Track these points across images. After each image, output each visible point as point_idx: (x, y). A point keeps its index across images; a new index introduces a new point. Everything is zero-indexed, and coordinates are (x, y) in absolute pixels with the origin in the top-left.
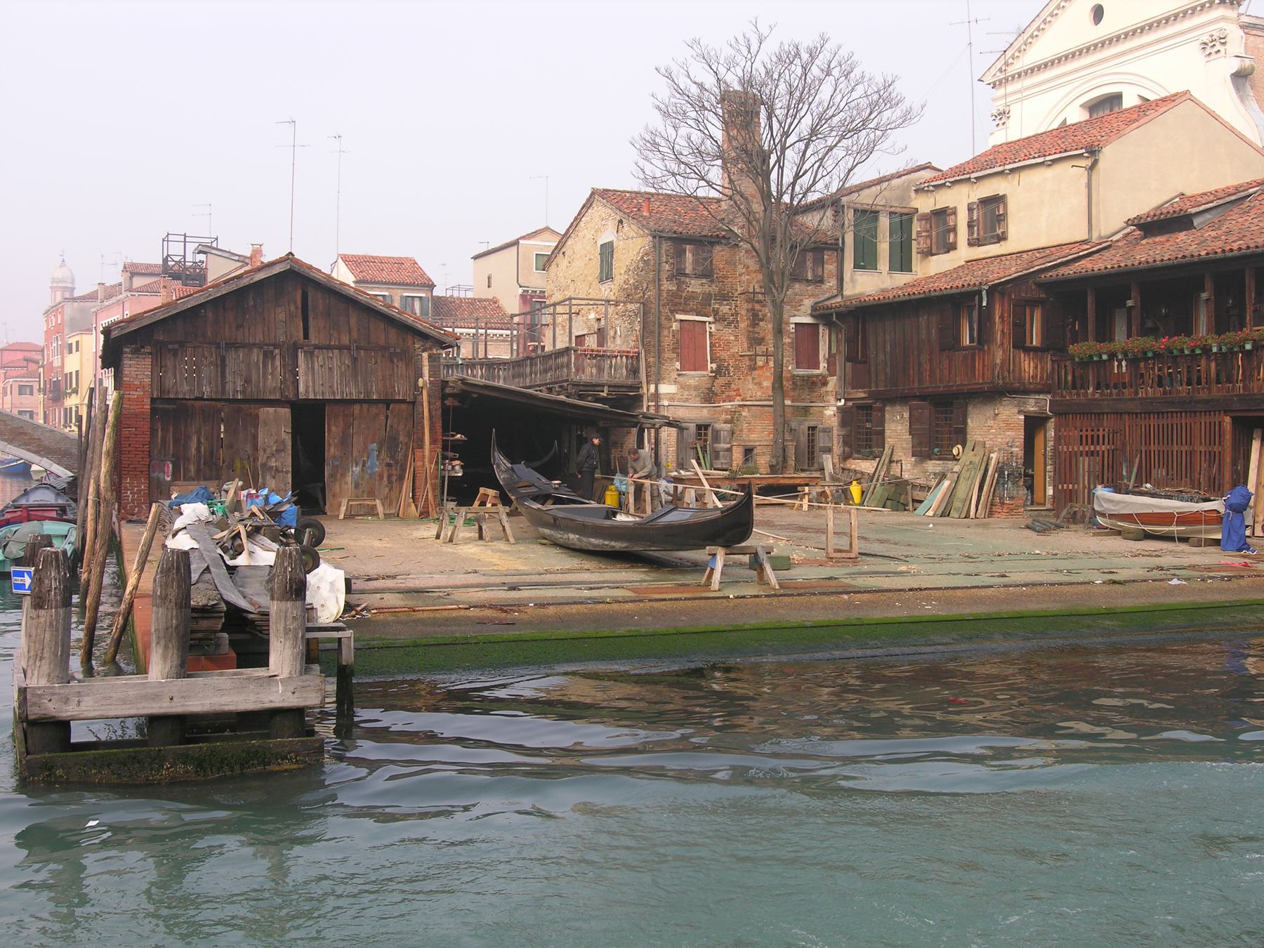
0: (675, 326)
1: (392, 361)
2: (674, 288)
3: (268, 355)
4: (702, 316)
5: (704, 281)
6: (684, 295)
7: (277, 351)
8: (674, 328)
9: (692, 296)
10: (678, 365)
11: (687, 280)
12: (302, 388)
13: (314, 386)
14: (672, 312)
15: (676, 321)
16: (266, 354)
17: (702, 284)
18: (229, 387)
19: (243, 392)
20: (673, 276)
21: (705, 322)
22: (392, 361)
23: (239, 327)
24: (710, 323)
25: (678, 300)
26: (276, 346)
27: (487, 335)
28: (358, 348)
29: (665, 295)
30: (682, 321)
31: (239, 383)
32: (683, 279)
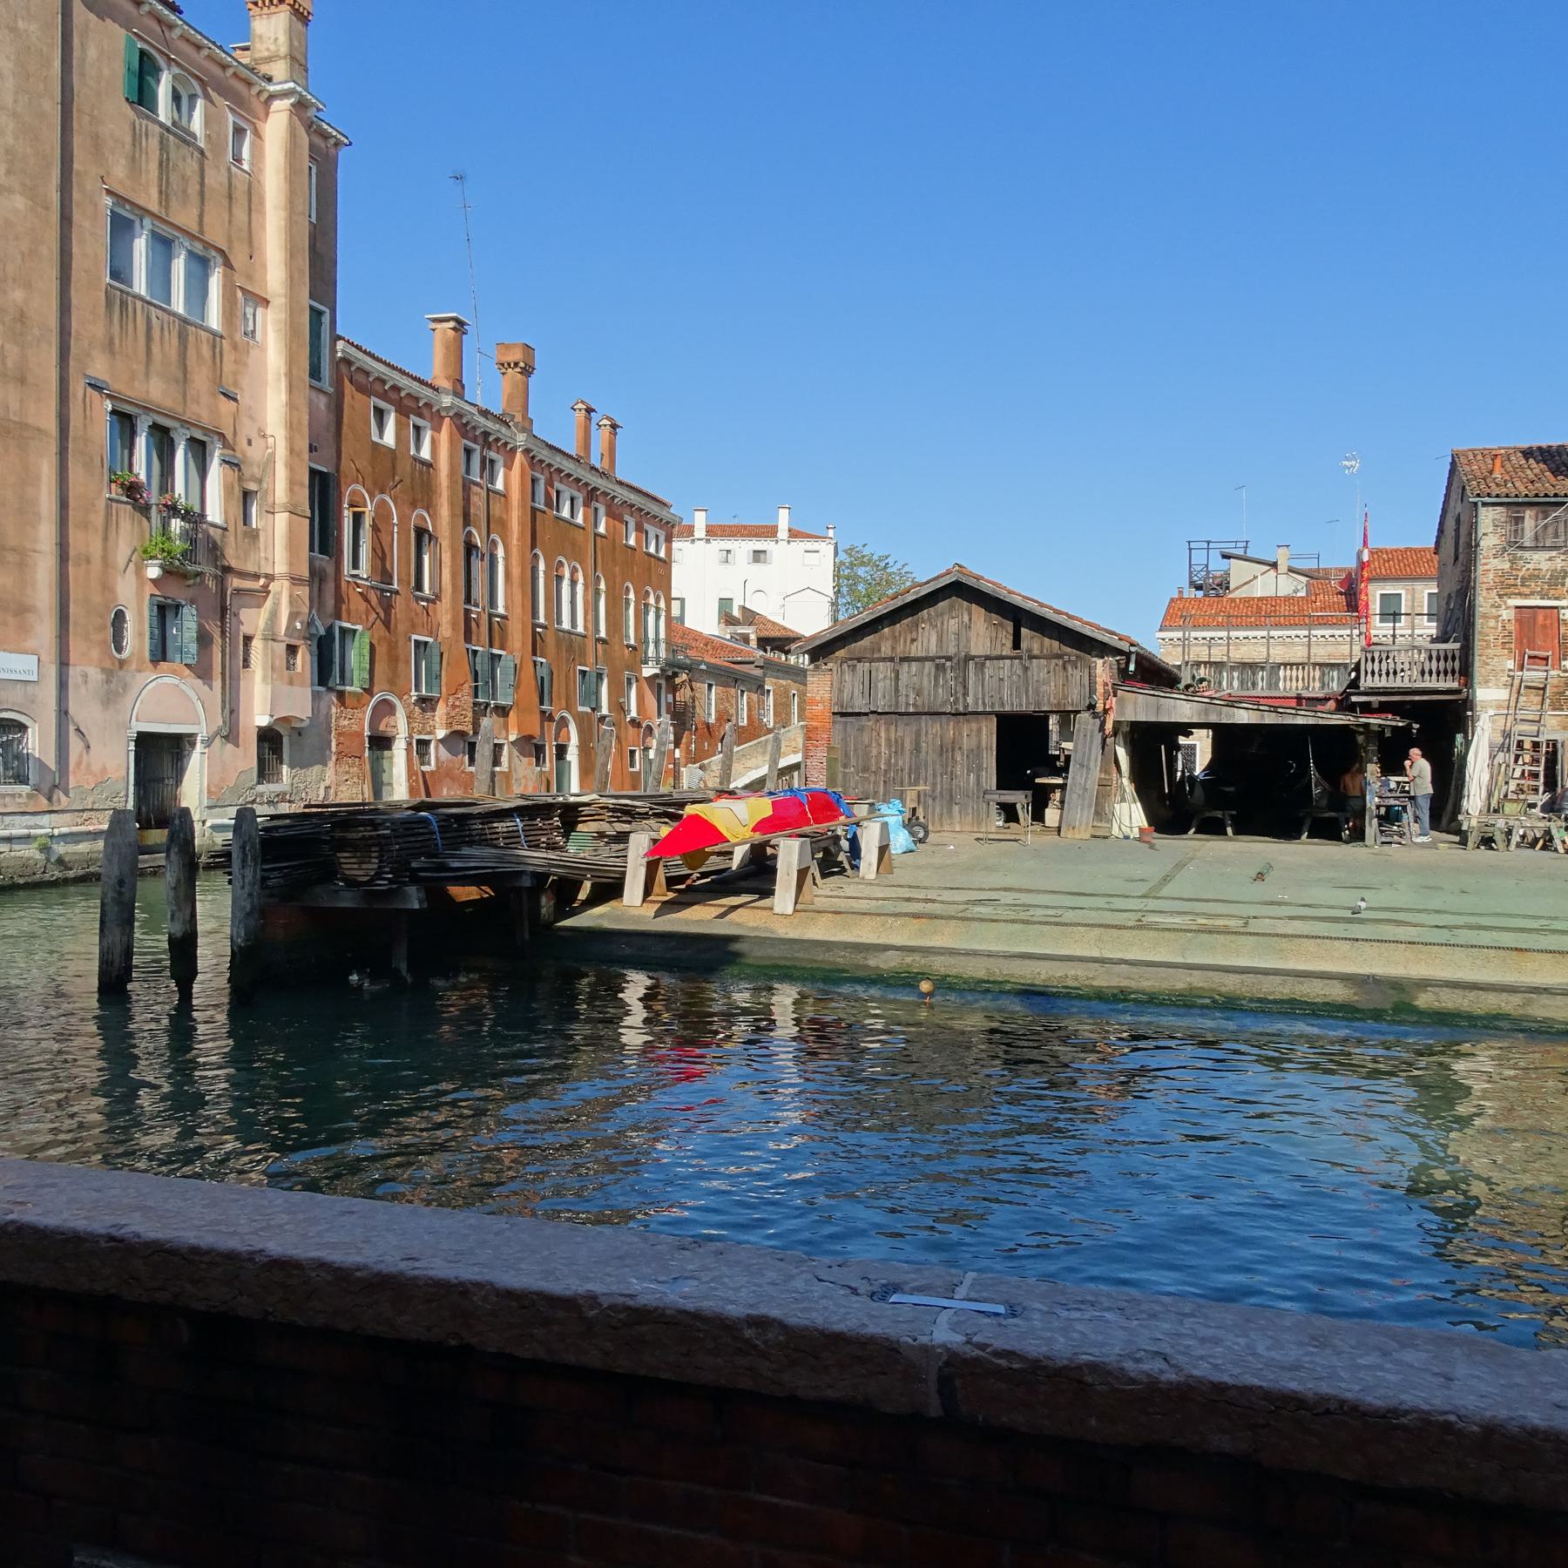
0: (1507, 614)
1: (1065, 668)
2: (1507, 566)
3: (940, 668)
4: (1549, 599)
5: (1554, 553)
6: (1521, 574)
7: (948, 664)
8: (1504, 617)
9: (1534, 576)
10: (1510, 664)
11: (1527, 554)
12: (970, 700)
13: (983, 699)
14: (1500, 596)
15: (1507, 608)
16: (937, 667)
17: (1550, 559)
18: (902, 699)
19: (914, 705)
20: (1504, 550)
21: (1556, 608)
22: (1065, 668)
23: (913, 640)
24: (1563, 608)
25: (1512, 582)
26: (949, 659)
27: (1229, 638)
28: (1031, 657)
29: (1491, 575)
30: (1517, 607)
31: (912, 696)
32: (1520, 553)
